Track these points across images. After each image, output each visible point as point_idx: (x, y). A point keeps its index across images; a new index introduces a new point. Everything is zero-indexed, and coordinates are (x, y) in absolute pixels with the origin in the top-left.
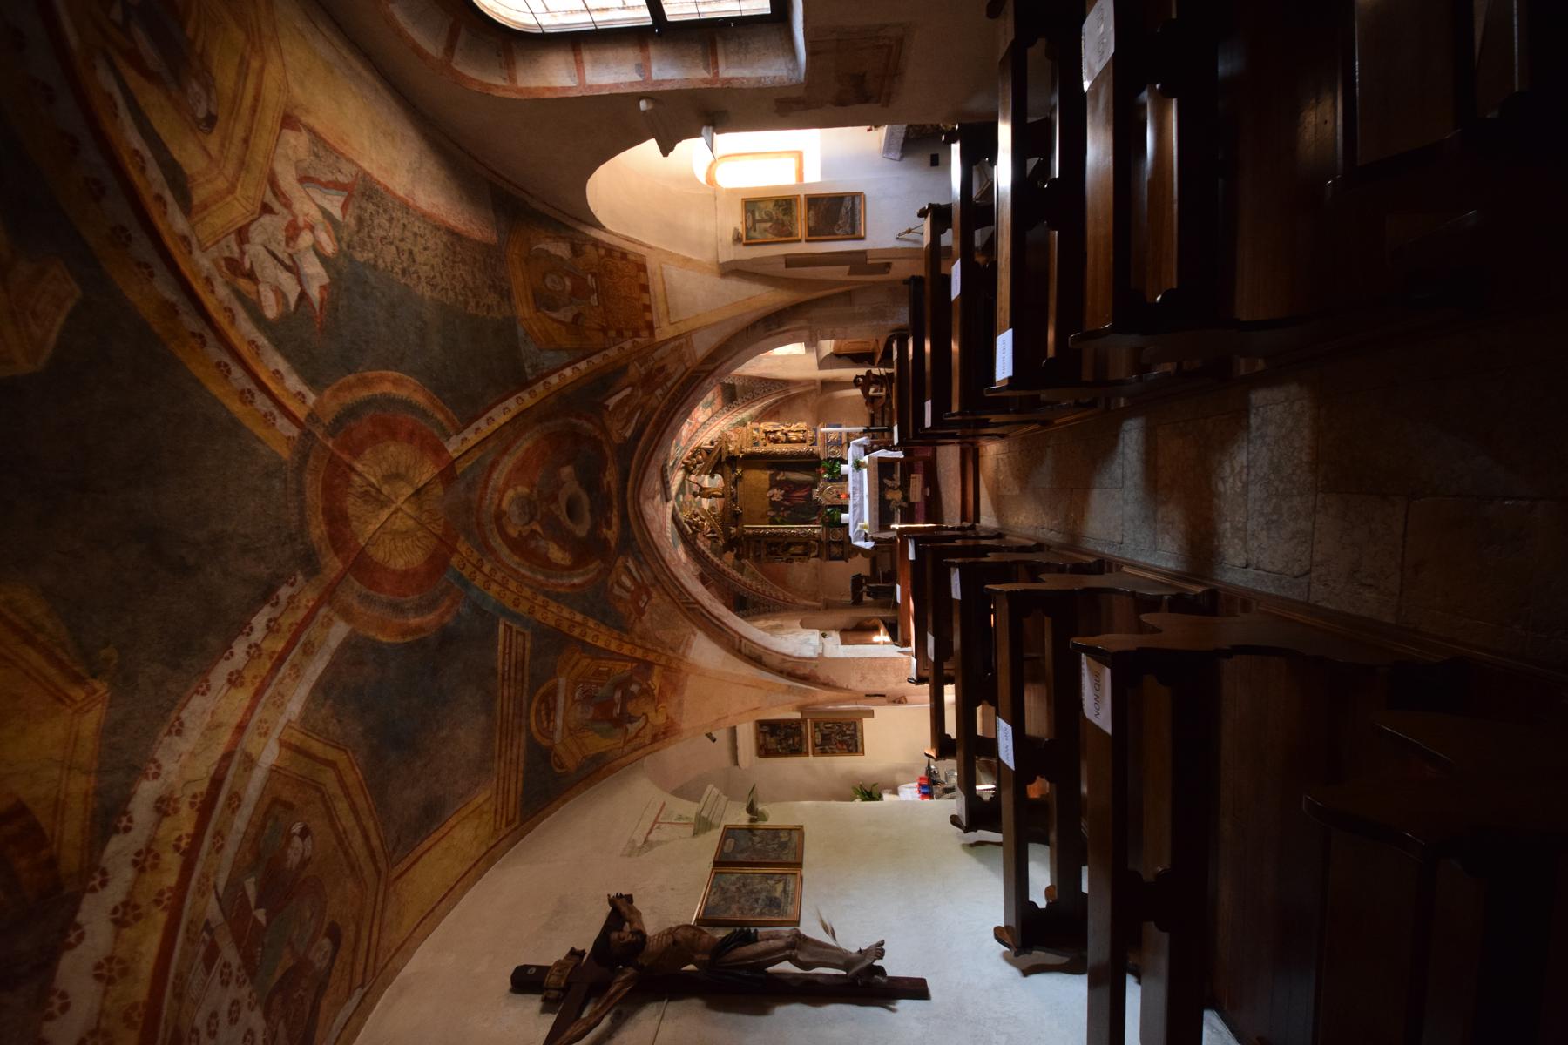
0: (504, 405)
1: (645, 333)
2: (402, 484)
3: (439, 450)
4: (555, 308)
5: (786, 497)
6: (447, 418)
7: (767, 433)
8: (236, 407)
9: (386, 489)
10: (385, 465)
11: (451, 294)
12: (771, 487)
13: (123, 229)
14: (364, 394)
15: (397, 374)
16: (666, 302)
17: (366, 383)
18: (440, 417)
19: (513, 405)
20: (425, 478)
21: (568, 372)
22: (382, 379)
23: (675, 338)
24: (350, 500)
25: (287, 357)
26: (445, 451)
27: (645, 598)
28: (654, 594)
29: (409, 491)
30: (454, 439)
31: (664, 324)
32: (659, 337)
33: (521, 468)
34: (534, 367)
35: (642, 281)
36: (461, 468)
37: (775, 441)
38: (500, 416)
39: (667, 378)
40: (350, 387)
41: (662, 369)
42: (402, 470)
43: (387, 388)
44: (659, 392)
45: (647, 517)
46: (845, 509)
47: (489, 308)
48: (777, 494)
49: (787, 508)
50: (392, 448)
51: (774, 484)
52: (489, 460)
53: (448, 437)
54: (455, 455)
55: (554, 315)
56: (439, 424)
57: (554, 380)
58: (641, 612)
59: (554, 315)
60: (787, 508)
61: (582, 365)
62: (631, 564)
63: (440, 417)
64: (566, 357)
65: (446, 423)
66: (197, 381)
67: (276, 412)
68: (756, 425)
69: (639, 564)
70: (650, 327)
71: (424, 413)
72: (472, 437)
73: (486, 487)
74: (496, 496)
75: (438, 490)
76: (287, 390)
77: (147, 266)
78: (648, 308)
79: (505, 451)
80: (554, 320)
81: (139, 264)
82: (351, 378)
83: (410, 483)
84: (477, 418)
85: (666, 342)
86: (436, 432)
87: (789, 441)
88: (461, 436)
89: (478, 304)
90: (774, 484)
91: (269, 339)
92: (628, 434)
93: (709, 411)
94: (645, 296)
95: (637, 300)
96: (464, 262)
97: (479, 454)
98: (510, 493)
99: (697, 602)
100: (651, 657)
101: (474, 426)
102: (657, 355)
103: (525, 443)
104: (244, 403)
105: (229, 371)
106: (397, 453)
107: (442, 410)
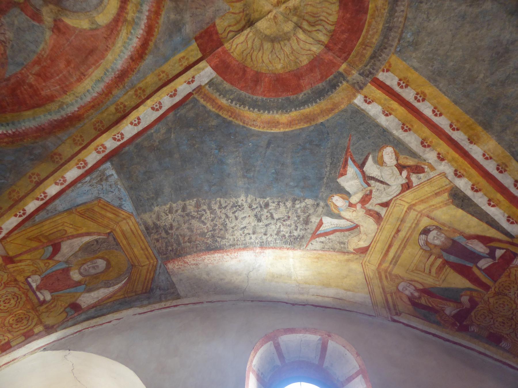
0: (140, 128)
2: (268, 32)
3: (224, 68)
4: (86, 248)
6: (213, 101)
8: (430, 90)
9: (288, 27)
10: (287, 50)
11: (216, 207)
13: (501, 172)
14: (307, 110)
15: (275, 130)
17: (308, 118)
18: (223, 101)
19: (128, 130)
20: (241, 38)
21: (52, 190)
22: (290, 123)
24: (333, 18)
25: (378, 125)
26: (215, 68)
29: (262, 25)
30: (206, 80)
33: (89, 53)
34: (103, 178)
36: (193, 51)
38: (146, 114)
40: (323, 112)
42: (267, 46)
43: (283, 118)
47: (171, 211)
50: (279, 66)
52: (149, 59)
53: (211, 83)
54: (203, 64)
55: (86, 239)
56: (223, 93)
57: (72, 174)
59: (86, 239)
61: (31, 206)
63: (223, 101)
64: (60, 205)
65: (216, 95)
66: (456, 103)
67: (397, 89)
71: (242, 102)
72: (182, 87)
73: (150, 30)
74: (130, 15)
75: (221, 25)
76: (380, 104)
77: (487, 159)
79: (122, 76)
80: (88, 234)
81: (491, 158)
82: (321, 120)
83: (258, 32)
84: (175, 107)
86: (227, 85)
88: (194, 85)
89: (184, 209)
91: (391, 134)
96: (203, 234)
97: (166, 67)
98: (104, 18)
101: (177, 99)
103: (89, 87)
104: (423, 93)
105: (434, 111)
106: (273, 61)
107: (220, 107)
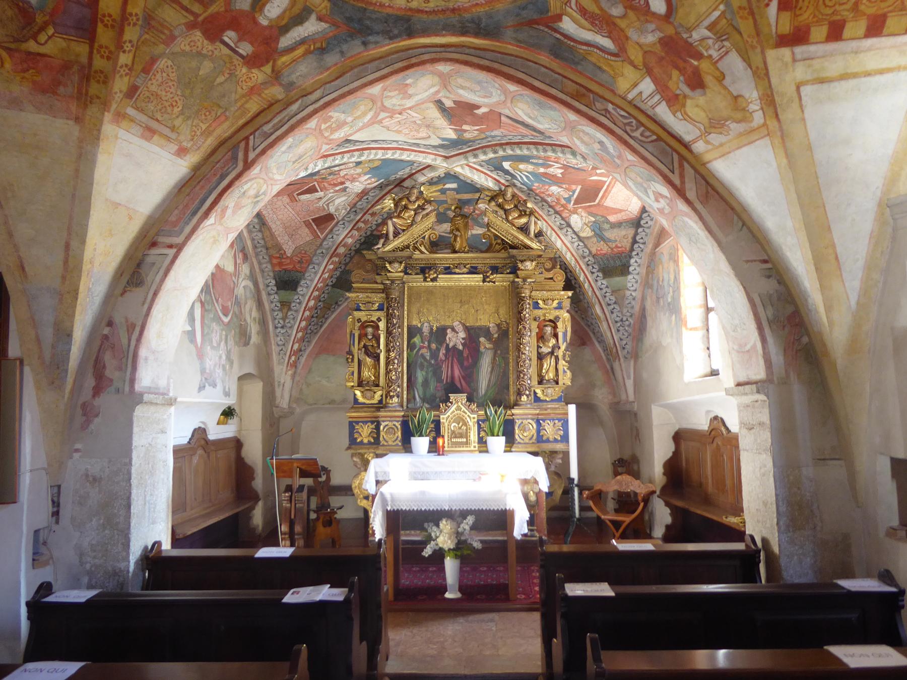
1: (786, 25)
5: (452, 352)
7: (554, 323)
12: (467, 329)
16: (844, 77)
23: (770, 101)
27: (246, 49)
28: (259, 75)
31: (800, 72)
32: (778, 57)
35: (891, 23)
37: (541, 337)
39: (674, 101)
41: (696, 82)
44: (647, 86)
45: (409, 78)
46: (434, 448)
48: (457, 338)
49: (434, 355)
51: (473, 334)
58: (212, 30)
60: (434, 355)
62: (311, 27)
68: (567, 304)
69: (319, 48)
70: (797, 37)
78: (836, 33)
85: (762, 75)
87: (541, 357)
90: (473, 334)
92: (567, 25)
93: (587, 233)
94: (861, 26)
95: (855, 8)
99: (248, 166)
100: (104, 36)
102: (734, 63)
